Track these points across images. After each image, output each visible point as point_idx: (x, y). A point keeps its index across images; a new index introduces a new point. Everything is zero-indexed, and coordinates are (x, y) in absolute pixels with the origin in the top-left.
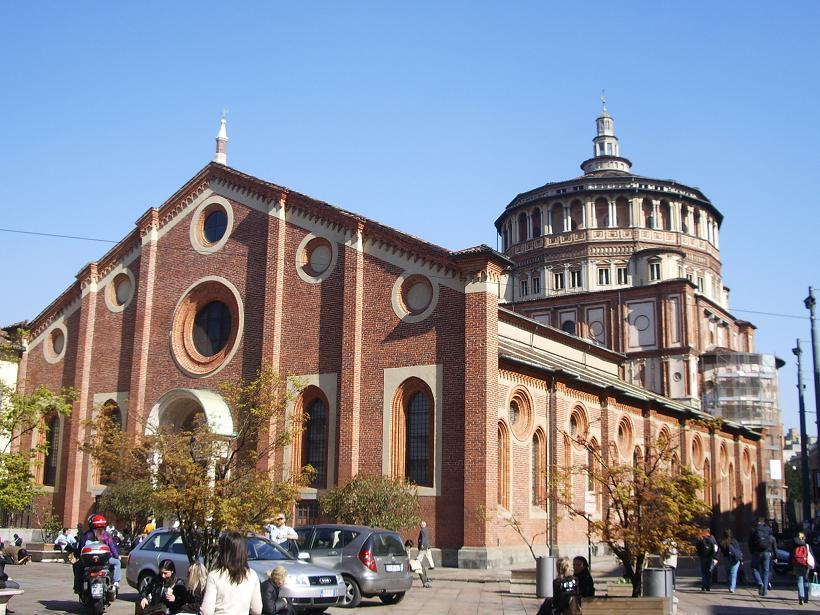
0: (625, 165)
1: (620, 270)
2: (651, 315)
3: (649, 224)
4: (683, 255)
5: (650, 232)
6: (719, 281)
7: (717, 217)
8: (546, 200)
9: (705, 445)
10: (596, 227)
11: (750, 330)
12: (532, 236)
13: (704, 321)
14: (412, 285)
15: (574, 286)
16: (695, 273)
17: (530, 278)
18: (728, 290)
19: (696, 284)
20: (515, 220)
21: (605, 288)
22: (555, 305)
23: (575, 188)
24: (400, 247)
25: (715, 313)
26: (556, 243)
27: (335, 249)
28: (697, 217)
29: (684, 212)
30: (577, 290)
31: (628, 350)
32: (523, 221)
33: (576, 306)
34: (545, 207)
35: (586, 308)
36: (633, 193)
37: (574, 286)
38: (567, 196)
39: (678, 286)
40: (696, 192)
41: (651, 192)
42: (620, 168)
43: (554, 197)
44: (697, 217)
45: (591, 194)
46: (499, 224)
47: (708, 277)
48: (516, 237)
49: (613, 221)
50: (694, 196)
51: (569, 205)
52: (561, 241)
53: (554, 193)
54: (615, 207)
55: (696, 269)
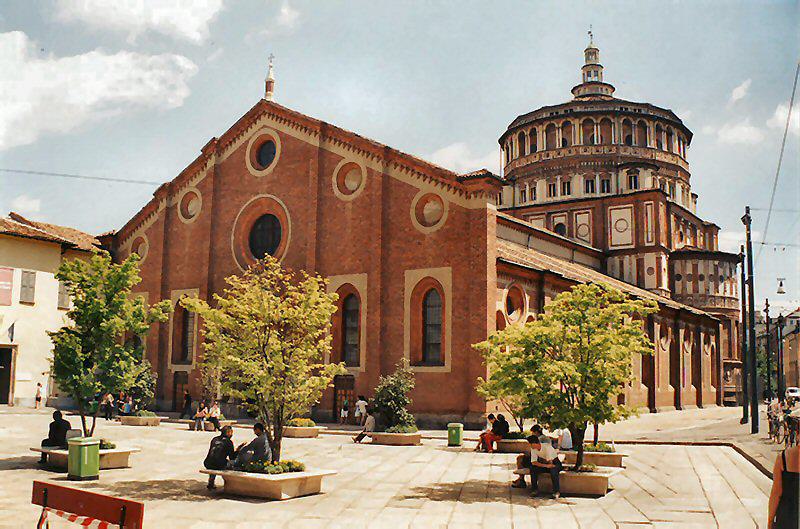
0: (610, 90)
3: (628, 141)
5: (630, 149)
7: (687, 136)
8: (540, 122)
17: (528, 187)
18: (697, 196)
20: (515, 137)
22: (547, 210)
23: (566, 111)
24: (416, 171)
26: (551, 157)
27: (365, 174)
28: (670, 134)
29: (658, 130)
30: (566, 197)
31: (611, 248)
32: (522, 138)
34: (540, 126)
36: (614, 114)
38: (559, 117)
40: (669, 112)
41: (630, 114)
44: (670, 134)
46: (502, 141)
47: (678, 187)
48: (516, 153)
50: (667, 118)
52: (552, 155)
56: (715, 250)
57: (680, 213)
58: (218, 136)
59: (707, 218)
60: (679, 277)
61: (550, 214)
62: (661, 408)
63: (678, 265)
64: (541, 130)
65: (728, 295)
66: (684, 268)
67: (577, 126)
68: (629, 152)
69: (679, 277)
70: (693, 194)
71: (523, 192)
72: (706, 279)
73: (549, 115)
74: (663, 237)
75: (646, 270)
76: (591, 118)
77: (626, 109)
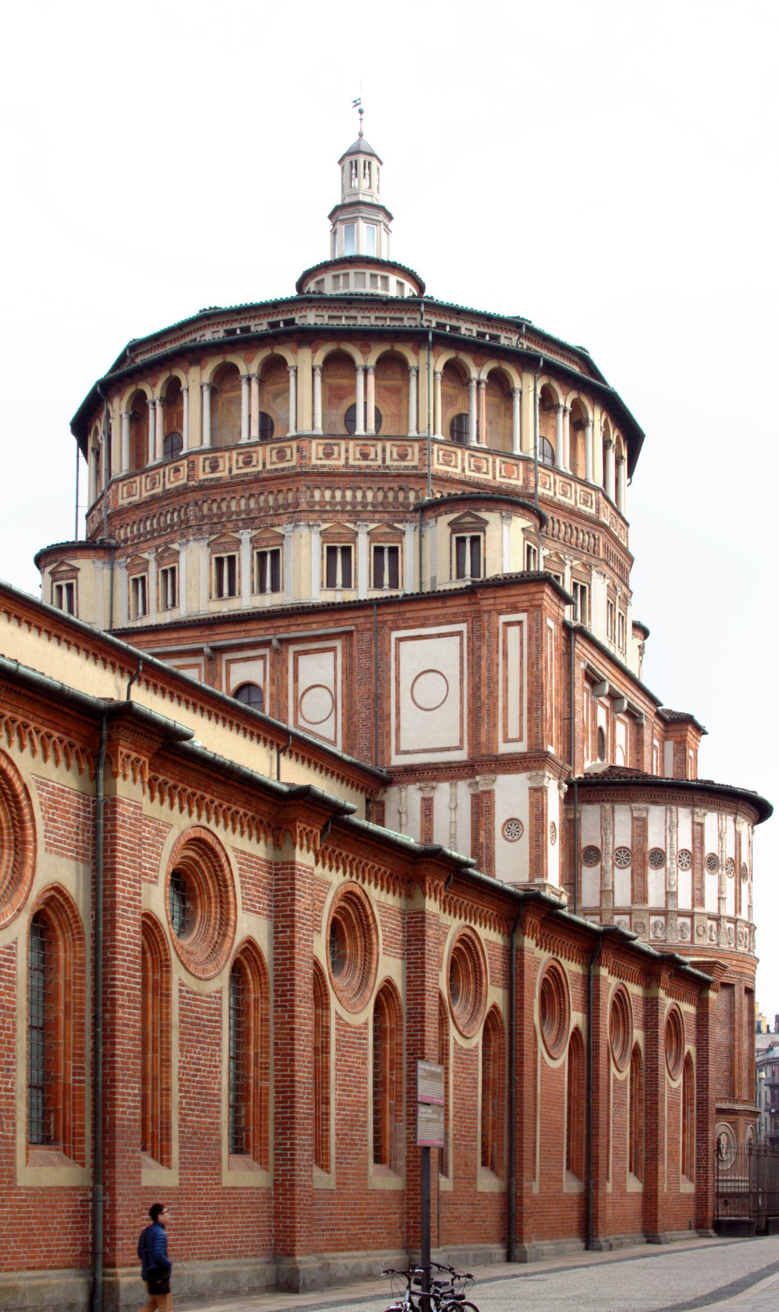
1: (379, 551)
4: (542, 520)
9: (574, 994)
11: (690, 733)
13: (581, 694)
18: (645, 633)
19: (568, 589)
25: (613, 681)
26: (222, 473)
47: (599, 588)
48: (121, 461)
57: (604, 669)
59: (672, 703)
60: (593, 855)
62: (546, 1246)
63: (590, 815)
66: (606, 825)
69: (593, 855)
70: (637, 626)
72: (671, 863)
73: (221, 334)
74: (553, 726)
75: (500, 818)
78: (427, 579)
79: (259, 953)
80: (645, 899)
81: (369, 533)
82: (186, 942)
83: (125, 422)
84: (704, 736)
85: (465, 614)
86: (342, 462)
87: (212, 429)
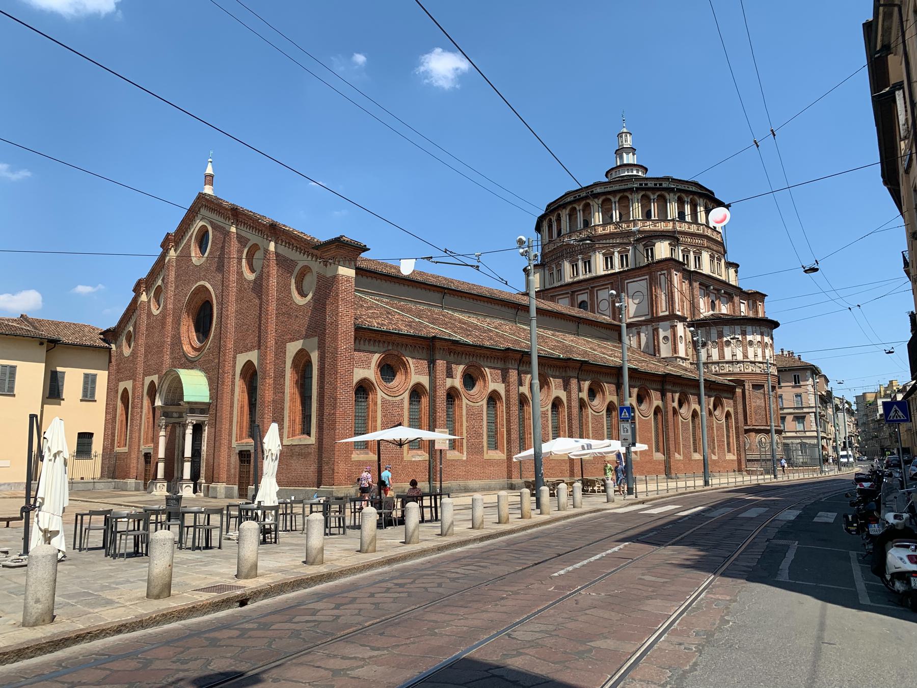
1: (622, 257)
2: (645, 291)
3: (647, 215)
6: (719, 260)
8: (564, 206)
10: (601, 223)
12: (556, 236)
14: (305, 275)
15: (586, 272)
16: (692, 253)
17: (555, 268)
21: (609, 272)
29: (681, 202)
30: (588, 276)
32: (550, 227)
33: (588, 289)
34: (564, 210)
35: (596, 289)
36: (631, 190)
37: (586, 272)
39: (670, 263)
42: (635, 173)
43: (570, 203)
45: (596, 196)
46: (538, 228)
47: (705, 256)
48: (547, 239)
49: (616, 216)
50: (694, 189)
51: (581, 207)
53: (572, 199)
54: (617, 205)
55: (692, 250)
56: (760, 315)
57: (707, 282)
58: (172, 230)
61: (573, 292)
64: (564, 214)
65: (760, 359)
67: (596, 206)
68: (649, 226)
71: (552, 274)
76: (610, 197)
77: (646, 184)
78: (637, 263)
79: (499, 394)
80: (724, 358)
81: (618, 252)
82: (472, 392)
83: (547, 228)
84: (766, 297)
85: (647, 273)
86: (609, 231)
87: (570, 227)
